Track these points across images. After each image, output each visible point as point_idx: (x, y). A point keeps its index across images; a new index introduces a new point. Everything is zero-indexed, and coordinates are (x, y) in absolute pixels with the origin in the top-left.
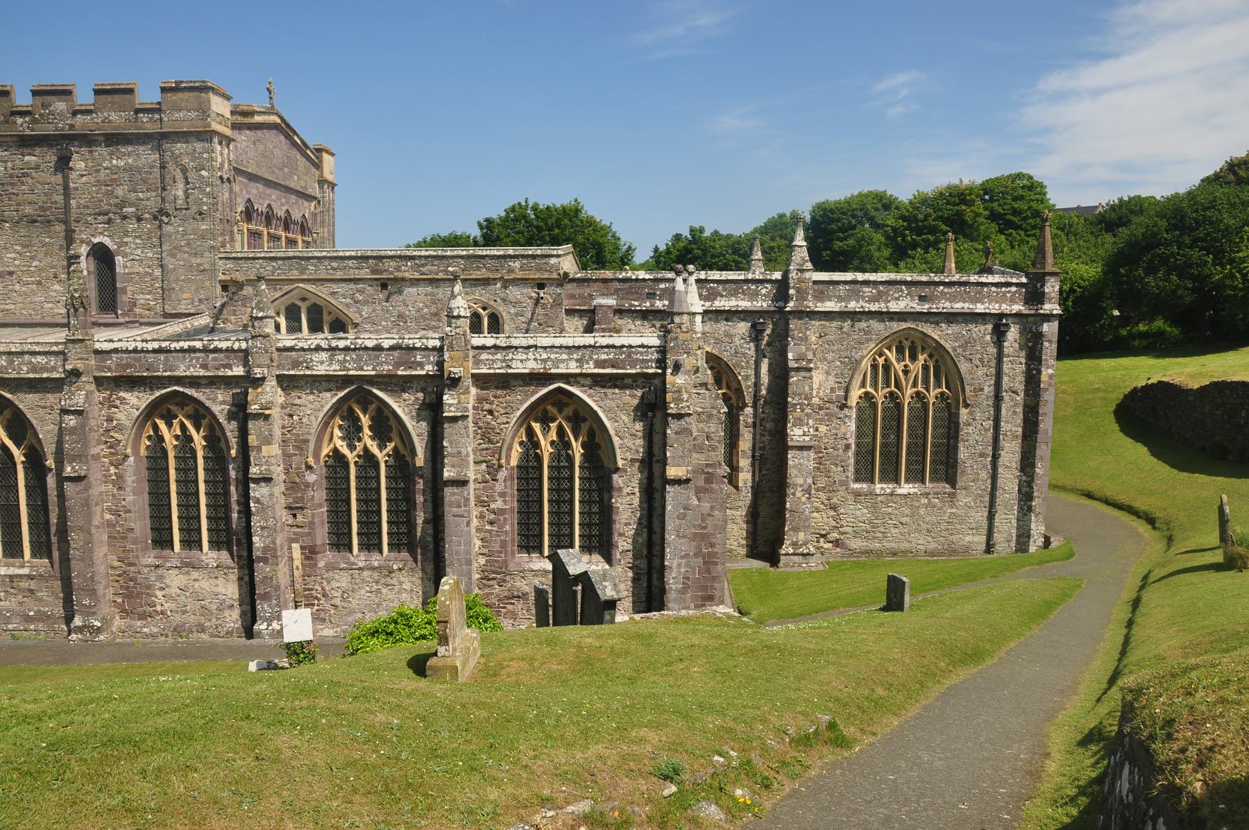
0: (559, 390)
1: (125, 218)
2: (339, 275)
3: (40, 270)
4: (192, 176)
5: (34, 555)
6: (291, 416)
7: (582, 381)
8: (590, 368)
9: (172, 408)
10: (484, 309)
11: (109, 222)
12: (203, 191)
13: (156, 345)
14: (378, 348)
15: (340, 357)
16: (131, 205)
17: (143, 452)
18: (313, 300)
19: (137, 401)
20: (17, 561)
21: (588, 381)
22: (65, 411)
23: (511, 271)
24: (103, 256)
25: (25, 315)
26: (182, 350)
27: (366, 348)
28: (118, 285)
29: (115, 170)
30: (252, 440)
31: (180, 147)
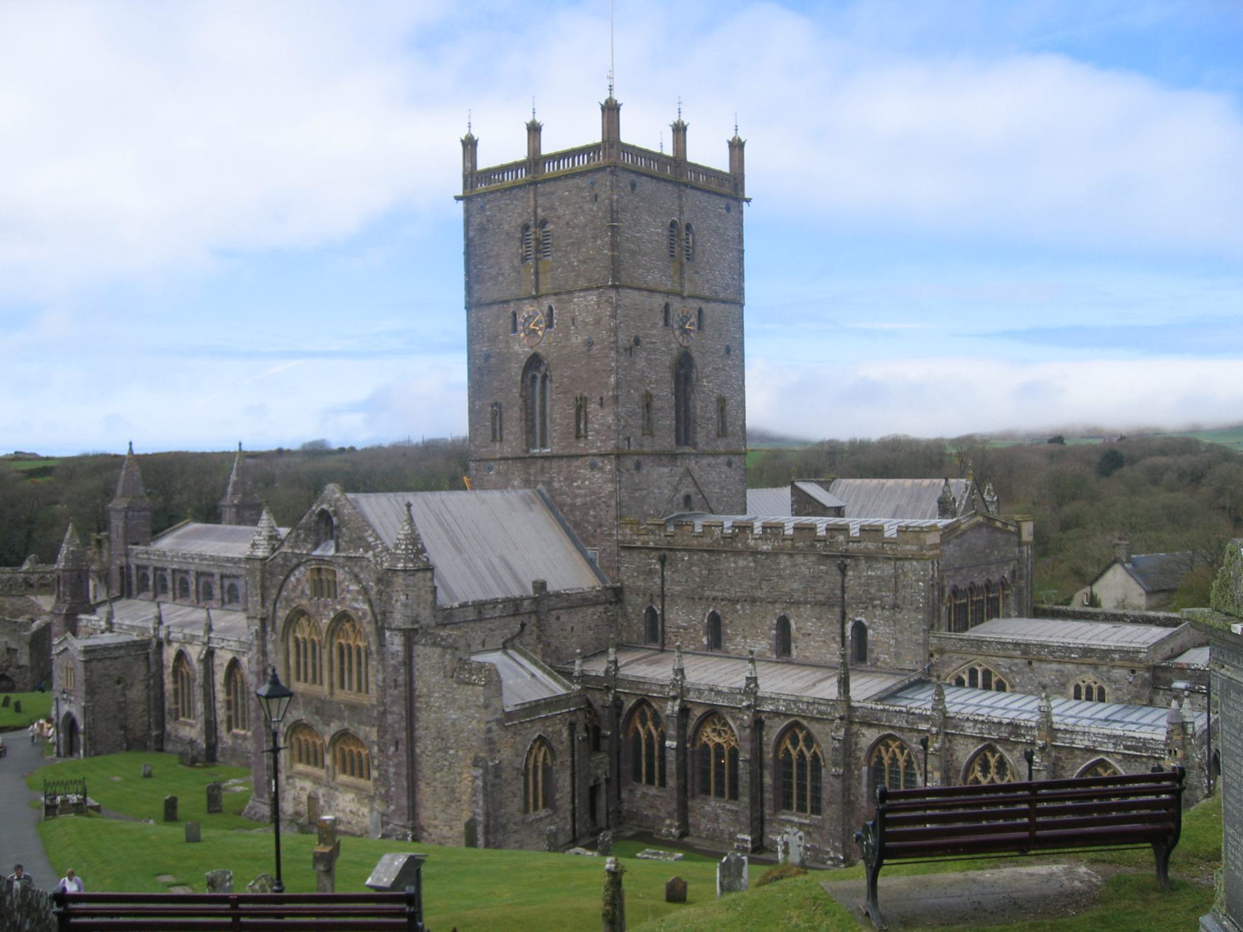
0: (1102, 761)
1: (874, 607)
2: (1001, 653)
3: (825, 634)
4: (914, 584)
5: (812, 812)
6: (952, 756)
7: (1116, 756)
8: (1121, 749)
9: (890, 742)
10: (1095, 683)
11: (866, 608)
12: (920, 595)
13: (880, 707)
14: (1000, 723)
15: (979, 726)
16: (878, 599)
17: (872, 764)
18: (985, 666)
19: (869, 736)
20: (804, 814)
21: (1120, 757)
22: (834, 739)
23: (1113, 660)
24: (860, 629)
25: (814, 659)
26: (896, 711)
27: (993, 723)
28: (869, 647)
29: (870, 577)
30: (929, 768)
31: (907, 564)
